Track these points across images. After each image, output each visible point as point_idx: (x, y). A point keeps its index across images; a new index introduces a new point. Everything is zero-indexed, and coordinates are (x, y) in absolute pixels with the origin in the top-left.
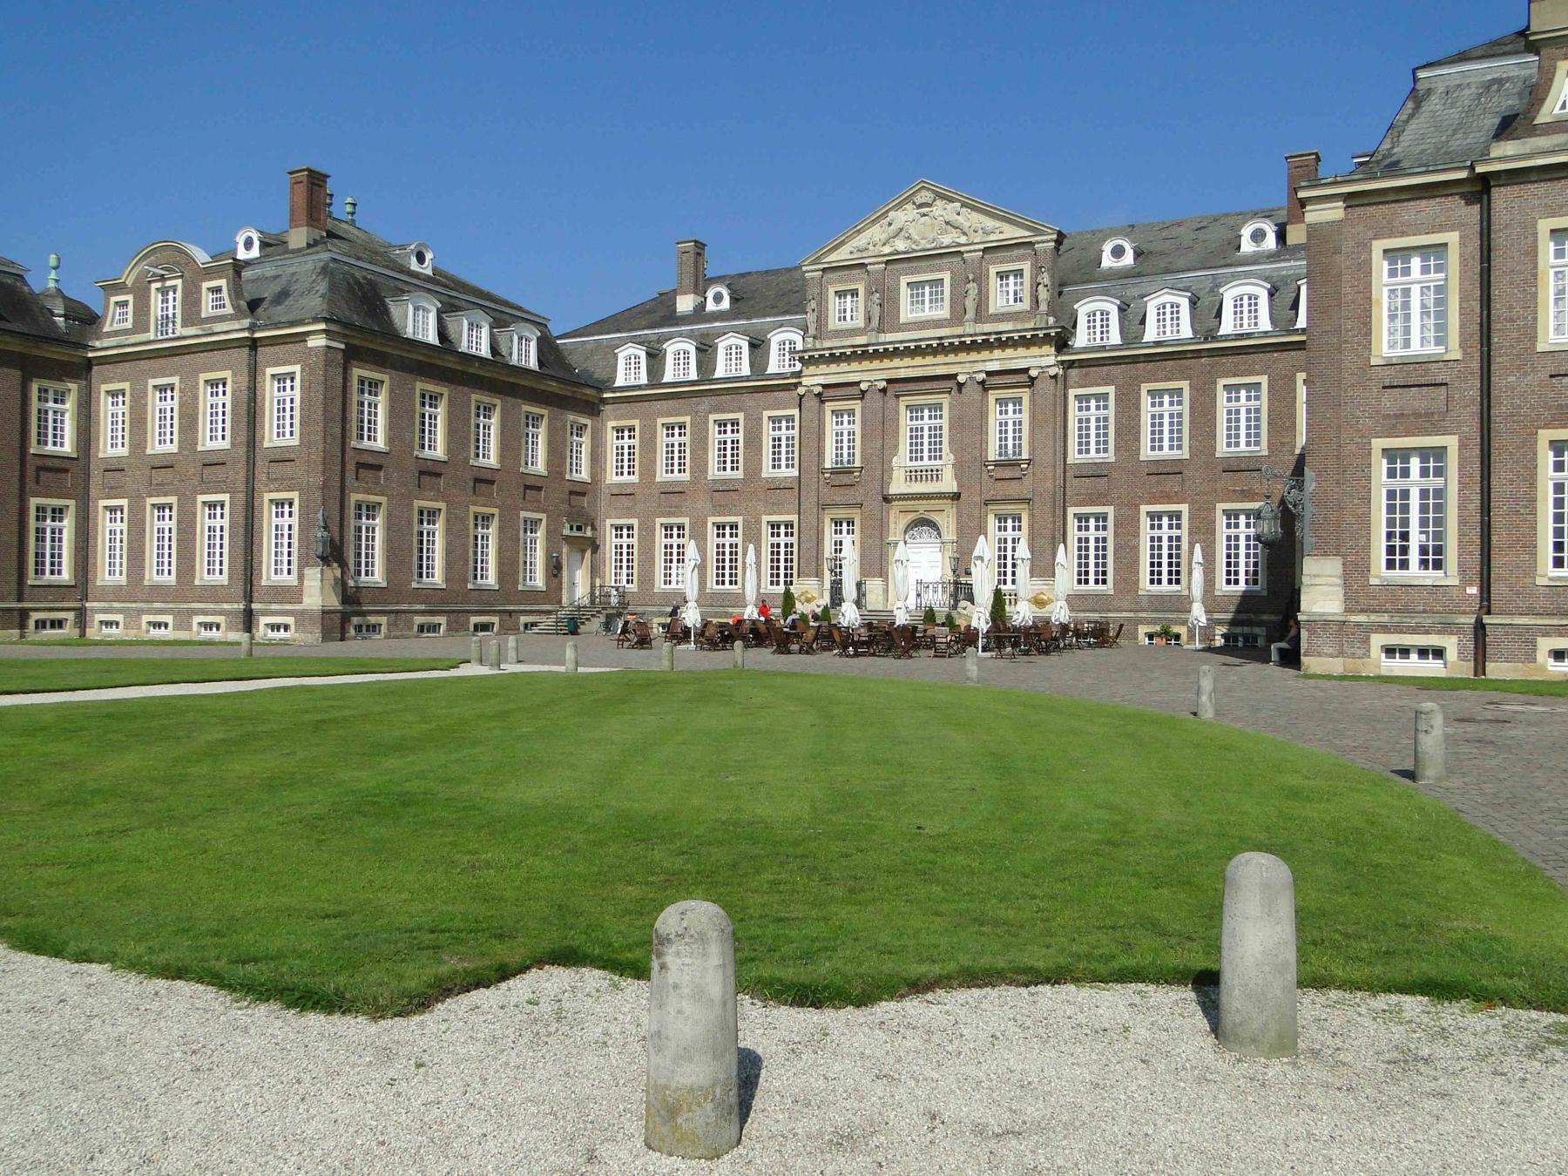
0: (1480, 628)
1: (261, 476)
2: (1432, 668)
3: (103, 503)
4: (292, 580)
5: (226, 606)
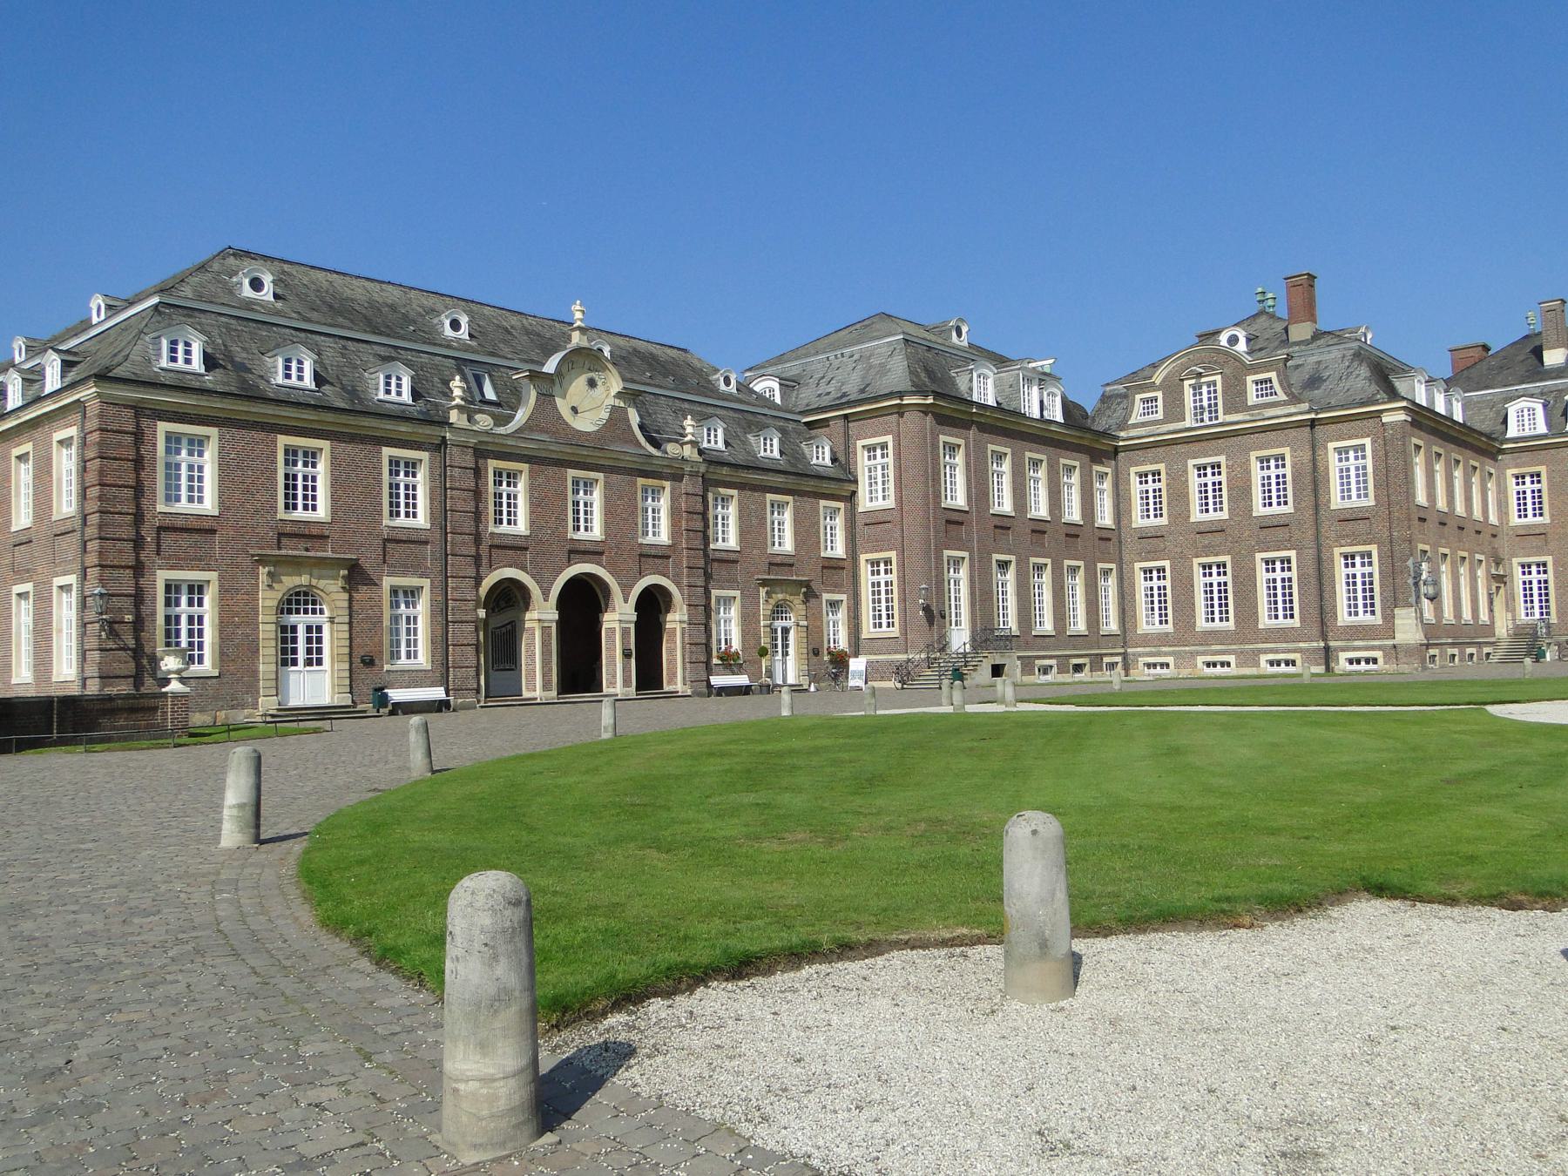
1: (1330, 530)
3: (1137, 565)
4: (1378, 619)
5: (1302, 645)
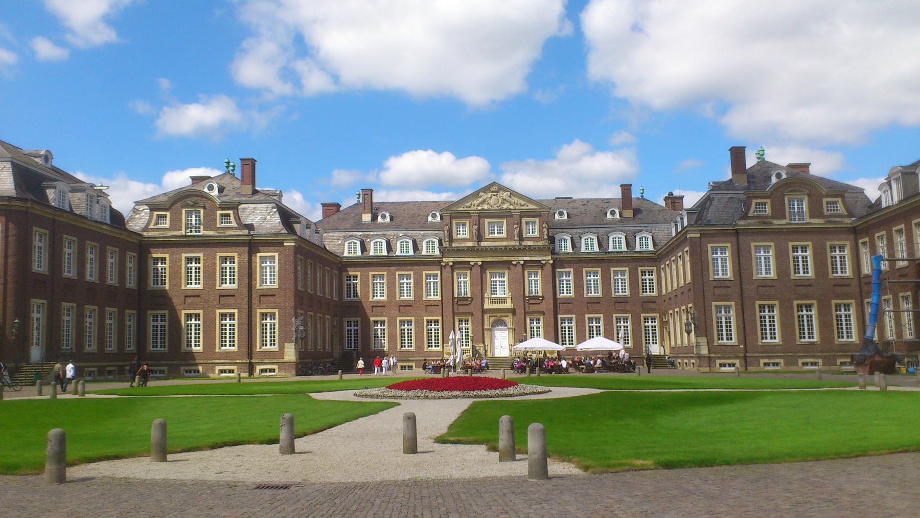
0: (745, 357)
1: (255, 301)
2: (732, 369)
4: (275, 348)
